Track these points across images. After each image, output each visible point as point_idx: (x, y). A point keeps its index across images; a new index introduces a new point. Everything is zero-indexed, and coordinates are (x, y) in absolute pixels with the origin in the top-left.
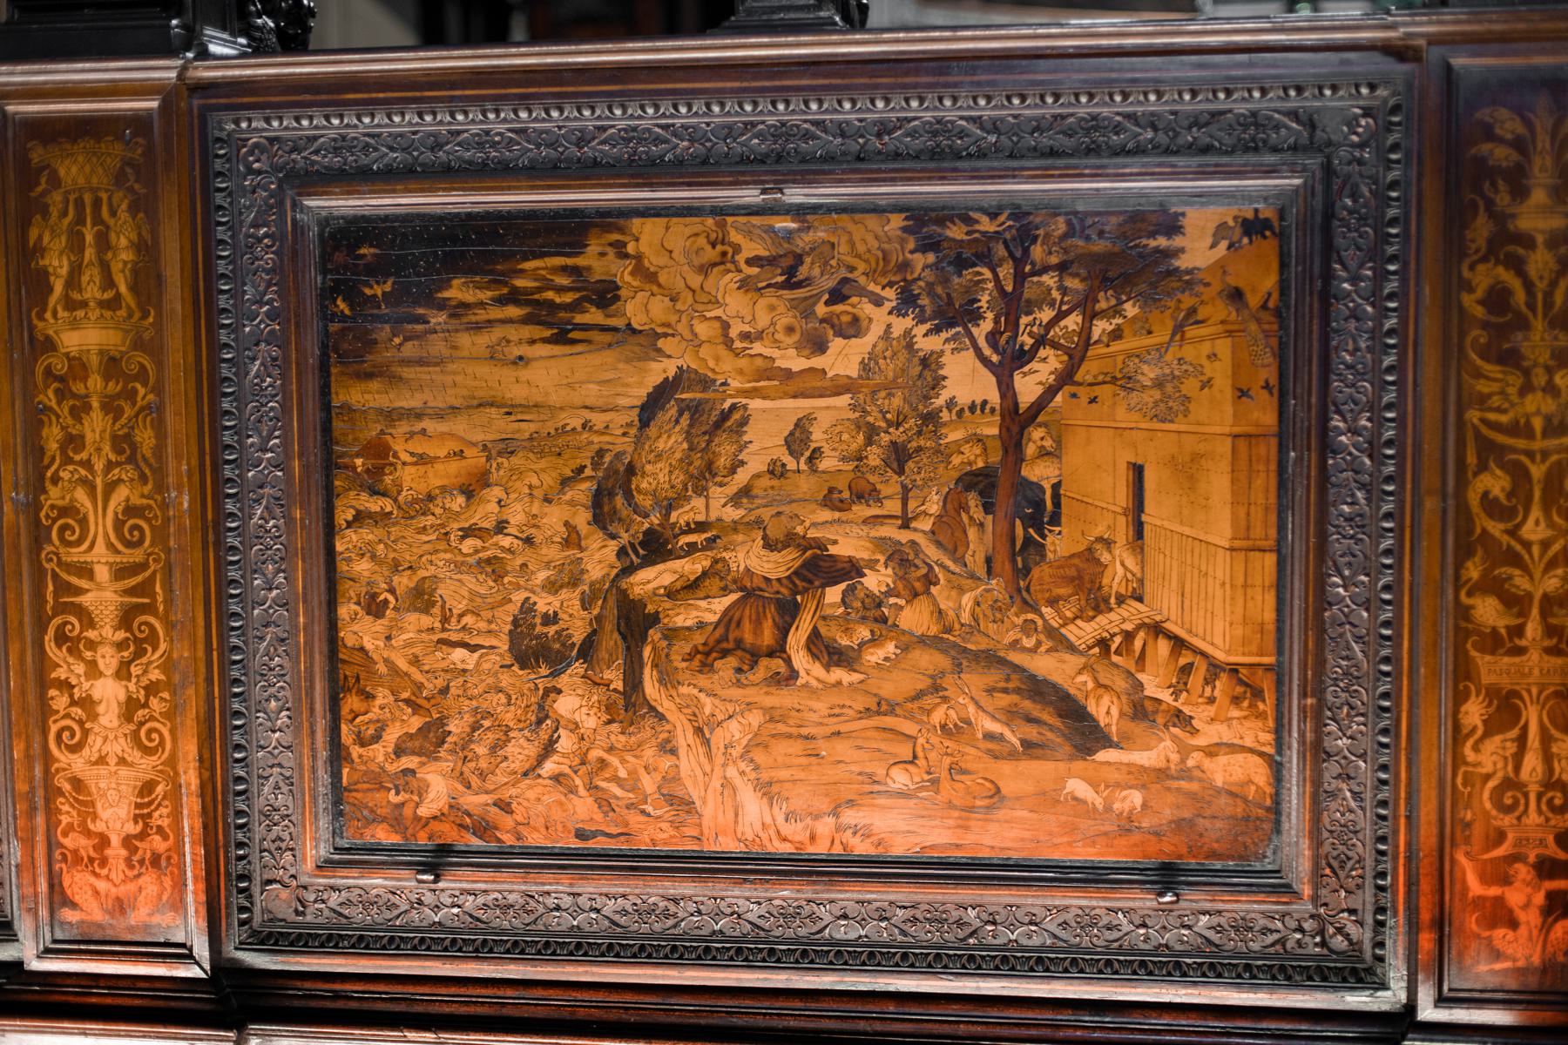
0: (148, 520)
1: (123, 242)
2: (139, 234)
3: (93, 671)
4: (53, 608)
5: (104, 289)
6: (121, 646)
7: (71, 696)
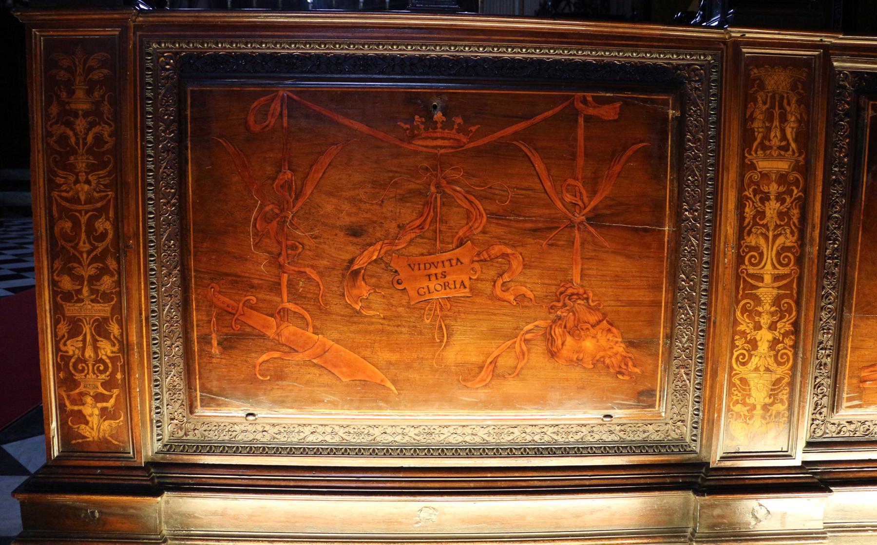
0: (793, 254)
1: (793, 119)
2: (801, 115)
3: (758, 327)
4: (742, 296)
5: (781, 141)
6: (772, 314)
7: (746, 338)
